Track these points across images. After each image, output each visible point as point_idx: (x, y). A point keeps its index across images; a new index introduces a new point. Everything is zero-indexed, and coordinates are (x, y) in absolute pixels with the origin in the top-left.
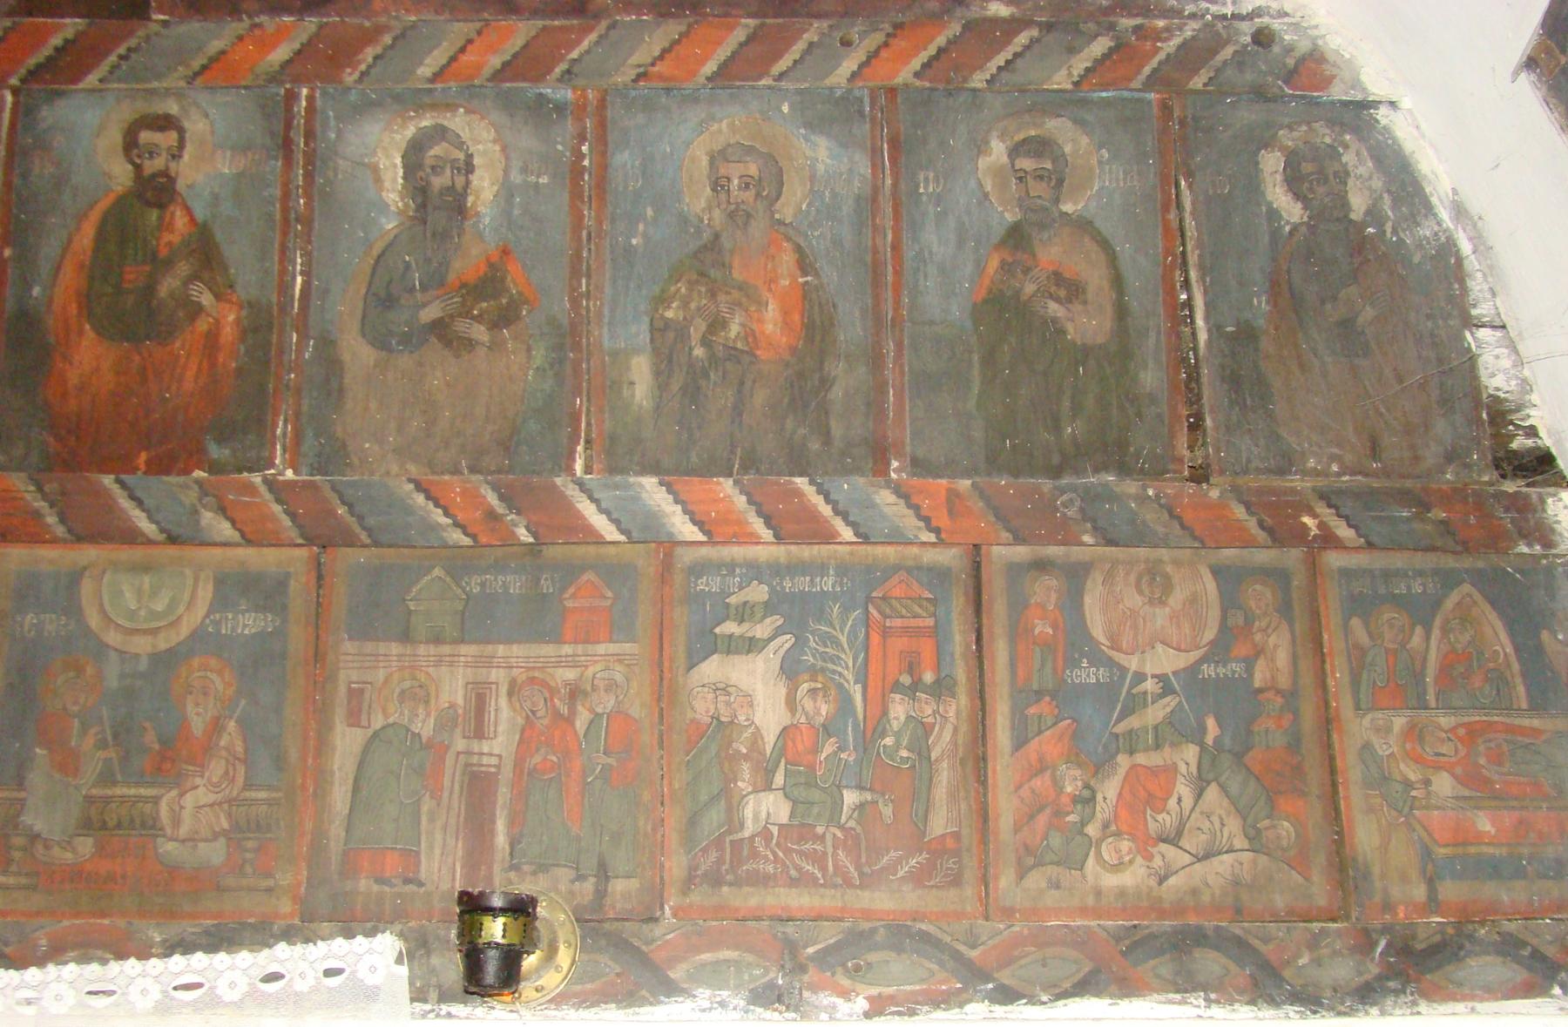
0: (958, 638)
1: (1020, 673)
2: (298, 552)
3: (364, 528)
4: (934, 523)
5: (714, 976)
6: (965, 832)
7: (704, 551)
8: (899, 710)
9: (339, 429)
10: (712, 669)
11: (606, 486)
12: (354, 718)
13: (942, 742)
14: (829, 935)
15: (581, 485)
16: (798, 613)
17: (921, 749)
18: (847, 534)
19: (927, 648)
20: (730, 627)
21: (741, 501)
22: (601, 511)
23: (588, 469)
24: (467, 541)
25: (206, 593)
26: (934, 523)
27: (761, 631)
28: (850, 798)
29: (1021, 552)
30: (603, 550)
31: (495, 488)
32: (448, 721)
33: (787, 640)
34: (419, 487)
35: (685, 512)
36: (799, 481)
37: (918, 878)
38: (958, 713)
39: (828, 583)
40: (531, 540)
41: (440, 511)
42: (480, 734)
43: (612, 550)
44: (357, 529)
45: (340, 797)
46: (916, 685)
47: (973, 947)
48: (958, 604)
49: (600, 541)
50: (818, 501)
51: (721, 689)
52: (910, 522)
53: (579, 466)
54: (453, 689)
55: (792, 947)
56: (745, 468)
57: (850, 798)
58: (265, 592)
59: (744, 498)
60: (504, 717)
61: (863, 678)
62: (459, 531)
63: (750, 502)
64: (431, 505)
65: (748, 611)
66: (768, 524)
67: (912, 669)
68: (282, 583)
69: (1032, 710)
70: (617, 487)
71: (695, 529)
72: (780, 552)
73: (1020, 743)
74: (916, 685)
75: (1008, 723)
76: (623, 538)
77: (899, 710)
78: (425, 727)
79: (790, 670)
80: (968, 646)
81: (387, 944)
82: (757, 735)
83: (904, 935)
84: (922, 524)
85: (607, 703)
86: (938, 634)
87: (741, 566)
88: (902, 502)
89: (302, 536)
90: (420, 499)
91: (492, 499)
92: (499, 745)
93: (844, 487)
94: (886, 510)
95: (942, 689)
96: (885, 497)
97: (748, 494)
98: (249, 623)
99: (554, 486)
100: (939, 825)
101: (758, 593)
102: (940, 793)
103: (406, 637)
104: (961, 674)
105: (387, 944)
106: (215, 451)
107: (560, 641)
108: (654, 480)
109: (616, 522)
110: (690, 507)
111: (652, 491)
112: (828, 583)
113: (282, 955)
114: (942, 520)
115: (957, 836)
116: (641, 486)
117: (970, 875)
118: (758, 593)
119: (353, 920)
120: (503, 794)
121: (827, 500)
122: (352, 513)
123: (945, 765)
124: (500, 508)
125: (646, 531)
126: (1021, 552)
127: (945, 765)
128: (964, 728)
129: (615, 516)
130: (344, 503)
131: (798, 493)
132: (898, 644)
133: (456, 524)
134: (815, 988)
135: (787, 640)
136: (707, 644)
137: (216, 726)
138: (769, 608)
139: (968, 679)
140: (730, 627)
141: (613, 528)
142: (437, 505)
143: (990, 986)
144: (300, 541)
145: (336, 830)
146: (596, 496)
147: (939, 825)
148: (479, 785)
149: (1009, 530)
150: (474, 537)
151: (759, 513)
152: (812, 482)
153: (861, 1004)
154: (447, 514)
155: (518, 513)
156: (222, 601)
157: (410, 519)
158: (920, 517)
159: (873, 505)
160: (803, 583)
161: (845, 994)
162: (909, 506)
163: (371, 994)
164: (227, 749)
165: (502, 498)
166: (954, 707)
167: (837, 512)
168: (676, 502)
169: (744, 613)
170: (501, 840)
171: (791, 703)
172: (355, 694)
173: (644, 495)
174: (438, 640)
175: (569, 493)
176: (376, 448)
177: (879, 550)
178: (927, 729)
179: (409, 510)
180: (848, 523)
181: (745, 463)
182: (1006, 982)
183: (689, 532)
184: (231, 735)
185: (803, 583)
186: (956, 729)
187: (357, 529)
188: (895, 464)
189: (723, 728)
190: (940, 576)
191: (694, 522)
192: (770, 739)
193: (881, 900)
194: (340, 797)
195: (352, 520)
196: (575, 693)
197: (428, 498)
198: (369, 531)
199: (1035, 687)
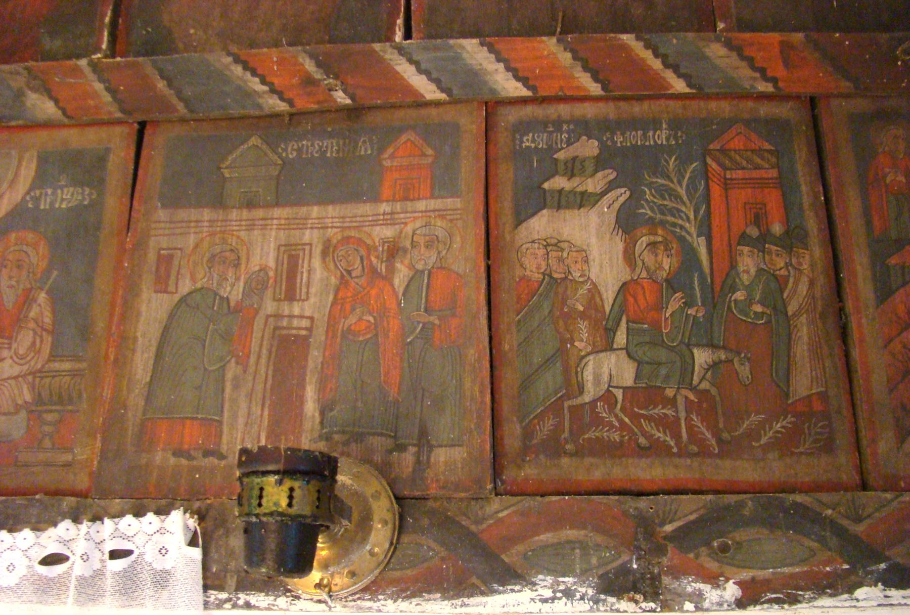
0: (804, 188)
1: (877, 223)
2: (118, 129)
3: (181, 99)
4: (770, 74)
5: (557, 561)
6: (831, 393)
7: (529, 111)
8: (748, 263)
9: (166, 17)
10: (541, 224)
11: (426, 49)
12: (162, 284)
13: (801, 292)
14: (689, 508)
15: (400, 50)
16: (630, 166)
17: (778, 307)
18: (679, 86)
19: (773, 200)
20: (559, 182)
21: (566, 58)
22: (420, 71)
23: (408, 35)
24: (282, 107)
25: (28, 171)
26: (770, 74)
27: (593, 185)
28: (702, 357)
29: (862, 105)
30: (424, 112)
31: (312, 56)
32: (258, 285)
33: (621, 195)
34: (237, 60)
35: (508, 69)
36: (624, 37)
37: (785, 444)
38: (812, 266)
39: (662, 136)
40: (348, 101)
41: (257, 80)
42: (291, 296)
43: (433, 112)
44: (174, 100)
45: (141, 365)
46: (765, 238)
47: (858, 520)
48: (801, 155)
49: (422, 104)
50: (647, 55)
51: (552, 245)
52: (744, 75)
53: (398, 36)
54: (264, 253)
55: (646, 526)
56: (564, 32)
57: (702, 357)
58: (86, 169)
59: (569, 55)
60: (317, 275)
61: (706, 230)
62: (275, 96)
63: (575, 58)
64: (248, 75)
65: (577, 164)
66: (596, 79)
67: (759, 219)
68: (101, 159)
69: (893, 261)
70: (436, 49)
71: (519, 85)
72: (609, 110)
73: (884, 293)
74: (765, 238)
75: (869, 273)
76: (443, 96)
77: (748, 263)
78: (235, 292)
79: (627, 223)
80: (816, 197)
81: (178, 522)
82: (595, 291)
83: (778, 507)
84: (757, 75)
85: (427, 259)
86: (785, 185)
87: (568, 122)
88: (734, 54)
89: (123, 111)
90: (238, 70)
91: (310, 66)
92: (312, 305)
93: (673, 42)
94: (717, 62)
95: (793, 239)
96: (716, 51)
97: (573, 51)
98: (66, 197)
99: (375, 51)
100: (803, 384)
101: (589, 148)
102: (801, 350)
103: (219, 202)
104: (813, 224)
105: (178, 522)
106: (49, 44)
107: (376, 199)
108: (475, 41)
109: (438, 82)
110: (512, 65)
111: (473, 52)
112: (662, 136)
113: (63, 534)
114: (779, 71)
115: (823, 397)
116: (463, 48)
117: (843, 440)
118: (589, 148)
119: (147, 500)
120: (315, 357)
121: (656, 55)
122: (170, 85)
123: (803, 319)
124: (318, 75)
125: (467, 90)
126: (862, 105)
127: (803, 319)
128: (821, 280)
129: (434, 76)
130: (162, 77)
131: (624, 47)
132: (741, 196)
133: (273, 91)
134: (677, 573)
135: (621, 195)
136: (534, 200)
137: (27, 299)
138: (600, 163)
139: (820, 229)
140: (559, 182)
141: (433, 87)
142: (254, 73)
143: (883, 566)
144: (118, 115)
145: (136, 400)
146: (415, 58)
147: (803, 384)
148: (289, 348)
149: (848, 79)
150: (291, 103)
151: (586, 69)
152: (638, 38)
153: (732, 591)
154: (263, 82)
155: (336, 77)
156: (41, 179)
157: (227, 89)
158: (753, 68)
159: (705, 58)
160: (635, 138)
161: (714, 579)
162: (742, 57)
163: (162, 579)
164: (36, 321)
165: (319, 65)
166: (807, 257)
167: (666, 65)
168: (499, 60)
169: (573, 168)
170: (311, 407)
171: (629, 257)
172: (165, 260)
173: (465, 55)
174: (250, 205)
175: (387, 56)
176: (200, 33)
177: (713, 105)
178: (781, 283)
179: (227, 81)
180: (680, 76)
181: (569, 27)
182: (899, 560)
183: (512, 88)
184: (41, 308)
185: (635, 138)
186: (812, 283)
187: (174, 100)
188: (721, 26)
189: (555, 285)
190: (776, 129)
191: (517, 78)
192: (609, 296)
193: (746, 471)
194: (141, 365)
195: (168, 92)
196: (394, 251)
197: (246, 68)
198: (186, 102)
199: (894, 235)
